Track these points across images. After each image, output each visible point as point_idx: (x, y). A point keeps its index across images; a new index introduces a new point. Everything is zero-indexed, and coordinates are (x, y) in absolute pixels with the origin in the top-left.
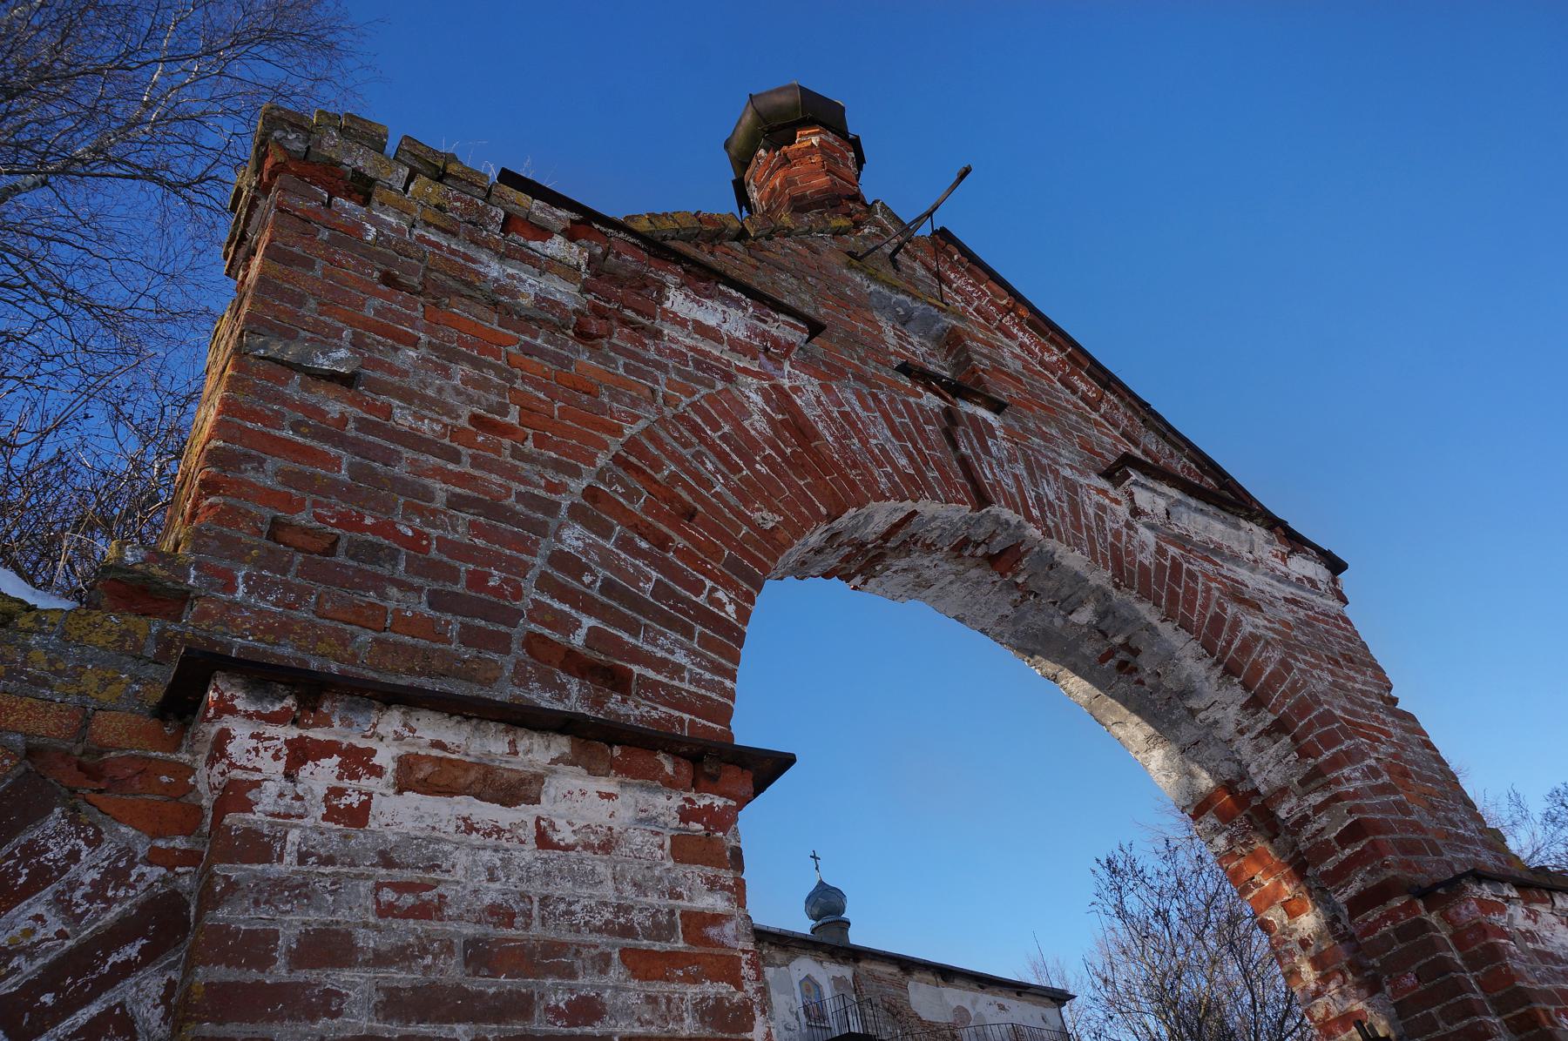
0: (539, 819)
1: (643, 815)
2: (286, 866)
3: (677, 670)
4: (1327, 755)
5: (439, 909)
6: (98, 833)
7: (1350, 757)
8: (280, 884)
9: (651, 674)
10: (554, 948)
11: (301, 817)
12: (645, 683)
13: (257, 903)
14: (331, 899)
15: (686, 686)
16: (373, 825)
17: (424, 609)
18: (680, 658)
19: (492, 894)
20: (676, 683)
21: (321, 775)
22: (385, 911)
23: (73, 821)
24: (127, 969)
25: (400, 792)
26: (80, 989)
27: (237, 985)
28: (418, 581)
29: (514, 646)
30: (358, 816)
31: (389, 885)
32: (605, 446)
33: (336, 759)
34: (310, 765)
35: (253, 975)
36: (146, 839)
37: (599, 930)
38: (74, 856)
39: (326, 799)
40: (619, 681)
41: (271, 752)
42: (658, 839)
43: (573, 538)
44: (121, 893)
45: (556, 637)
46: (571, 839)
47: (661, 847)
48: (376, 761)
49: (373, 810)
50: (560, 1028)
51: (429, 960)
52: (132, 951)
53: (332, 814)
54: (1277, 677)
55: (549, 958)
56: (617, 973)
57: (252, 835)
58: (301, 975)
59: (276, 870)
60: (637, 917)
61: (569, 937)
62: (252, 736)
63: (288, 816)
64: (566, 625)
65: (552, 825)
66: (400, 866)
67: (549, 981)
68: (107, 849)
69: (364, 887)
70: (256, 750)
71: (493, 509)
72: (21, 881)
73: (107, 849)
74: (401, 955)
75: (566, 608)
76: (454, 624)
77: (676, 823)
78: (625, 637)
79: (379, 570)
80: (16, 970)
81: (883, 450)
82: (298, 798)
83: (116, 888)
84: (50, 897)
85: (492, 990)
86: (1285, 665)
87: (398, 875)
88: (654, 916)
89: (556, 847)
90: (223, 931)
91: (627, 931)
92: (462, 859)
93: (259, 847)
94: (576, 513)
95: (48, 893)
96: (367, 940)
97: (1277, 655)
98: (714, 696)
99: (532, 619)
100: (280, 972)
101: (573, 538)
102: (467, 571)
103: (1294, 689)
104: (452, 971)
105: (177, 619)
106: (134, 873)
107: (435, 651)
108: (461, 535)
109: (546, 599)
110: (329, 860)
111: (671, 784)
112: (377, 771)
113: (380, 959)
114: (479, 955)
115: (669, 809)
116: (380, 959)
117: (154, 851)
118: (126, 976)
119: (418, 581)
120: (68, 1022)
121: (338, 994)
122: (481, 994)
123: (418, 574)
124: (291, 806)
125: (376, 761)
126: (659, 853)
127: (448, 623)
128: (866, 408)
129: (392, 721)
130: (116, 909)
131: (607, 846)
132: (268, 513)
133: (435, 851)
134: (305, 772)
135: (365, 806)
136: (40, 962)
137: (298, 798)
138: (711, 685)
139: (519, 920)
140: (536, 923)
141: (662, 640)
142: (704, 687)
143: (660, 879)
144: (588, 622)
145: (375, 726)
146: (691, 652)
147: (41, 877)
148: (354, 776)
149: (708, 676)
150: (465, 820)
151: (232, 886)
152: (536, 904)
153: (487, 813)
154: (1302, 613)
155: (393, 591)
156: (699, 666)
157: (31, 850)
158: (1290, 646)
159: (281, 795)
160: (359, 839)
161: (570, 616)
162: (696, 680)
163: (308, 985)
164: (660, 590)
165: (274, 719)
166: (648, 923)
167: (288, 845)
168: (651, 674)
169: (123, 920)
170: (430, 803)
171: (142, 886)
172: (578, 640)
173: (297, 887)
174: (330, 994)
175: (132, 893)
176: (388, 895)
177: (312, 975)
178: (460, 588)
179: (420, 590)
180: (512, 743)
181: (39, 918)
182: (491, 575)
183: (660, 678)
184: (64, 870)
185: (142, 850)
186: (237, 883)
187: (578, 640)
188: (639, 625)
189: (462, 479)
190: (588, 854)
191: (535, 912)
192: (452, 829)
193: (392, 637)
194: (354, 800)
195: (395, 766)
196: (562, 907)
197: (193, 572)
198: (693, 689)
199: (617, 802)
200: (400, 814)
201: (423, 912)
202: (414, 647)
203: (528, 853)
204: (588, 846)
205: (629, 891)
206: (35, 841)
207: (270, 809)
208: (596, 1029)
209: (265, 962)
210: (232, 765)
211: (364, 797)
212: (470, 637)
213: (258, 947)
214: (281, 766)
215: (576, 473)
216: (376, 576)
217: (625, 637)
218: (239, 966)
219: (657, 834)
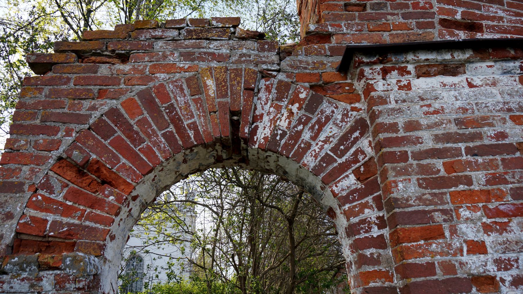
0: (467, 79)
1: (505, 71)
2: (393, 105)
3: (501, 18)
5: (442, 110)
6: (336, 105)
8: (393, 110)
9: (490, 23)
10: (484, 118)
11: (391, 90)
12: (488, 27)
13: (389, 115)
14: (409, 112)
15: (505, 24)
16: (413, 89)
17: (401, 20)
18: (501, 13)
19: (458, 104)
20: (501, 23)
21: (393, 77)
22: (426, 113)
23: (329, 103)
24: (357, 139)
25: (418, 78)
26: (348, 145)
27: (391, 137)
28: (396, 12)
29: (436, 25)
30: (408, 87)
31: (424, 106)
33: (396, 71)
34: (389, 75)
35: (395, 135)
36: (348, 105)
37: (499, 111)
38: (333, 112)
39: (397, 84)
40: (479, 28)
41: (377, 73)
42: (513, 78)
44: (348, 119)
45: (450, 18)
46: (480, 83)
47: (515, 81)
48: (408, 69)
49: (412, 85)
50: (494, 142)
51: (444, 125)
52: (357, 134)
53: (400, 88)
55: (484, 121)
56: (510, 123)
57: (380, 97)
58: (408, 134)
59: (390, 106)
60: (513, 106)
61: (489, 114)
62: (370, 69)
63: (388, 91)
65: (472, 79)
66: (427, 99)
67: (486, 129)
68: (340, 109)
69: (418, 107)
70: (372, 73)
72: (324, 119)
73: (340, 109)
74: (437, 125)
75: (451, 7)
76: (413, 22)
77: (519, 72)
78: (477, 12)
79: (383, 11)
80: (332, 142)
82: (388, 85)
83: (347, 118)
84: (332, 123)
85: (468, 132)
87: (426, 102)
88: (518, 104)
89: (476, 86)
90: (382, 125)
91: (510, 110)
92: (445, 94)
93: (383, 101)
95: (331, 122)
96: (424, 122)
98: (518, 25)
99: (439, 14)
100: (401, 134)
102: (411, 3)
104: (453, 128)
105: (331, 43)
106: (349, 114)
107: (409, 33)
109: (442, 5)
110: (404, 101)
111: (514, 59)
112: (409, 73)
113: (429, 127)
114: (459, 122)
115: (515, 67)
116: (429, 127)
117: (352, 107)
118: (358, 140)
119: (396, 12)
120: (349, 153)
121: (420, 138)
122: (464, 134)
123: (396, 9)
124: (387, 88)
125: (408, 69)
126: (515, 83)
127: (411, 23)
129: (410, 57)
130: (349, 124)
131: (494, 84)
132: (342, 3)
133: (435, 93)
134: (388, 77)
135: (409, 84)
136: (336, 139)
137: (388, 85)
138: (516, 22)
139: (470, 111)
140: (476, 111)
141: (491, 9)
142: (513, 23)
143: (517, 91)
144: (460, 10)
145: (405, 58)
146: (504, 11)
147: (328, 119)
148: (402, 75)
149: (514, 18)
150: (442, 83)
151: (380, 112)
152: (474, 105)
153: (449, 80)
155: (389, 17)
156: (510, 15)
157: (322, 112)
159: (384, 85)
160: (411, 94)
161: (453, 9)
162: (511, 21)
163: (410, 136)
165: (374, 63)
166: (517, 107)
167: (391, 99)
168: (490, 23)
169: (352, 127)
170: (429, 80)
171: (353, 118)
172: (458, 17)
173: (399, 109)
174: (418, 138)
175: (351, 119)
176: (425, 109)
177: (411, 133)
178: (411, 10)
179: (398, 14)
180: (452, 55)
181: (331, 128)
182: (420, 2)
183: (495, 23)
184: (332, 116)
185: (349, 109)
186: (381, 111)
187: (458, 17)
188: (480, 6)
190: (488, 87)
191: (475, 108)
192: (439, 86)
193: (394, 32)
194: (406, 83)
195: (414, 70)
196: (484, 105)
197: (330, 28)
198: (509, 25)
199: (494, 68)
200: (422, 84)
201: (436, 112)
202: (403, 34)
203: (467, 90)
204: (487, 85)
205: (508, 98)
206: (322, 110)
207: (382, 89)
208: (507, 141)
209: (397, 131)
210: (367, 79)
211: (408, 81)
212: (420, 26)
213: (393, 127)
214: (380, 77)
216: (382, 14)
217: (477, 12)
218: (390, 133)
219: (512, 76)
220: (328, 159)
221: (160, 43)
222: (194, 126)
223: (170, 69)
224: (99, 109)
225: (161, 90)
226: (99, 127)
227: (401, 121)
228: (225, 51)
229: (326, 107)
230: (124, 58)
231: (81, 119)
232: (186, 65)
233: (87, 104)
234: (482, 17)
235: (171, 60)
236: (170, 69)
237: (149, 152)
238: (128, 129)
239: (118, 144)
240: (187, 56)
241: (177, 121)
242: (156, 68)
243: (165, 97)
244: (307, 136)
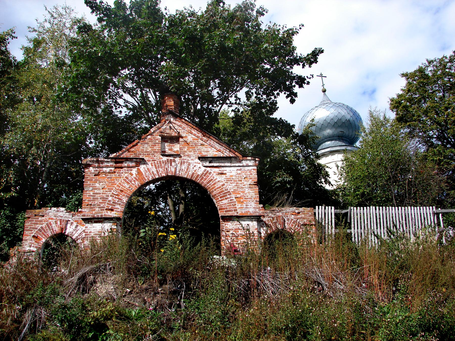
4: (220, 199)
7: (226, 199)
18: (119, 207)
32: (114, 187)
43: (110, 198)
54: (220, 187)
64: (109, 207)
71: (103, 198)
81: (153, 172)
86: (223, 185)
94: (111, 196)
97: (222, 184)
101: (110, 198)
103: (222, 189)
108: (101, 201)
128: (152, 165)
154: (239, 172)
158: (228, 180)
164: (118, 201)
189: (101, 196)
213: (87, 232)
215: (111, 191)
220: (77, 237)
221: (50, 213)
222: (55, 230)
223: (52, 219)
224: (39, 226)
225: (50, 223)
226: (39, 230)
227: (89, 231)
228: (62, 215)
229: (79, 227)
230: (43, 216)
231: (36, 229)
232: (55, 218)
233: (37, 225)
234: (115, 208)
235: (52, 217)
236: (52, 219)
237: (48, 235)
238: (44, 231)
239: (43, 233)
240: (55, 216)
241: (53, 229)
242: (49, 219)
243: (51, 225)
244: (74, 232)
